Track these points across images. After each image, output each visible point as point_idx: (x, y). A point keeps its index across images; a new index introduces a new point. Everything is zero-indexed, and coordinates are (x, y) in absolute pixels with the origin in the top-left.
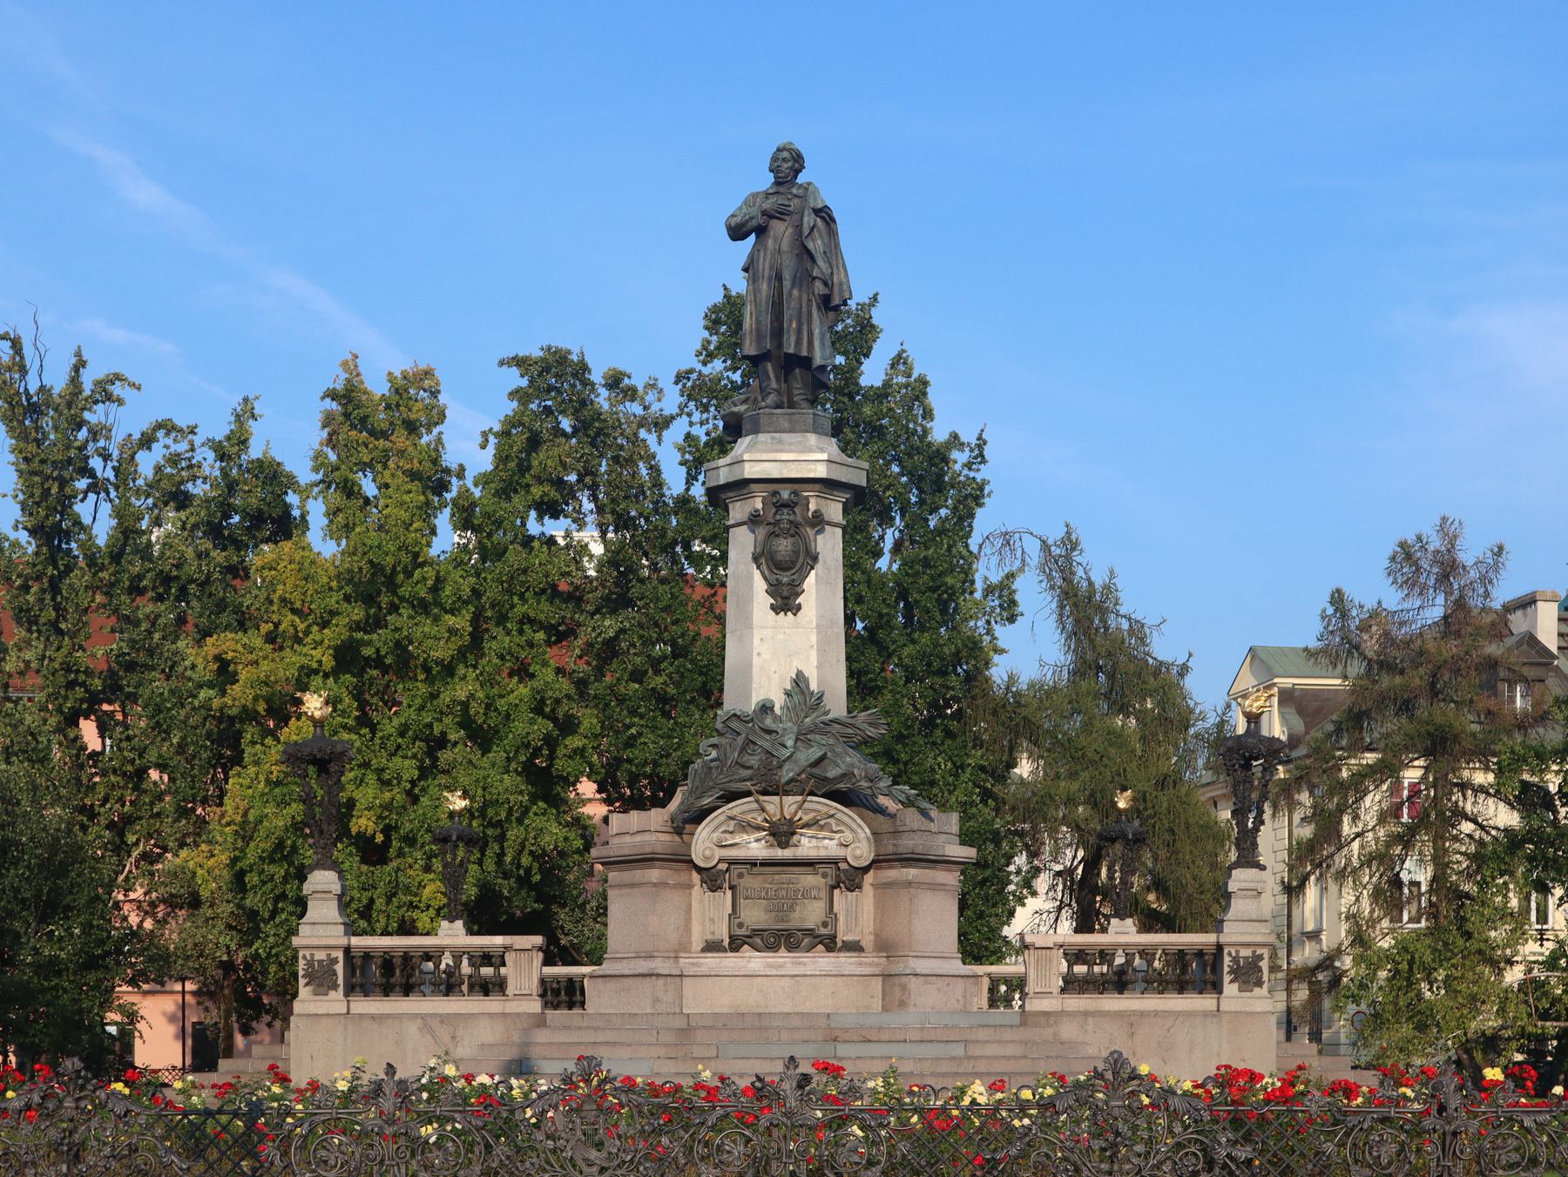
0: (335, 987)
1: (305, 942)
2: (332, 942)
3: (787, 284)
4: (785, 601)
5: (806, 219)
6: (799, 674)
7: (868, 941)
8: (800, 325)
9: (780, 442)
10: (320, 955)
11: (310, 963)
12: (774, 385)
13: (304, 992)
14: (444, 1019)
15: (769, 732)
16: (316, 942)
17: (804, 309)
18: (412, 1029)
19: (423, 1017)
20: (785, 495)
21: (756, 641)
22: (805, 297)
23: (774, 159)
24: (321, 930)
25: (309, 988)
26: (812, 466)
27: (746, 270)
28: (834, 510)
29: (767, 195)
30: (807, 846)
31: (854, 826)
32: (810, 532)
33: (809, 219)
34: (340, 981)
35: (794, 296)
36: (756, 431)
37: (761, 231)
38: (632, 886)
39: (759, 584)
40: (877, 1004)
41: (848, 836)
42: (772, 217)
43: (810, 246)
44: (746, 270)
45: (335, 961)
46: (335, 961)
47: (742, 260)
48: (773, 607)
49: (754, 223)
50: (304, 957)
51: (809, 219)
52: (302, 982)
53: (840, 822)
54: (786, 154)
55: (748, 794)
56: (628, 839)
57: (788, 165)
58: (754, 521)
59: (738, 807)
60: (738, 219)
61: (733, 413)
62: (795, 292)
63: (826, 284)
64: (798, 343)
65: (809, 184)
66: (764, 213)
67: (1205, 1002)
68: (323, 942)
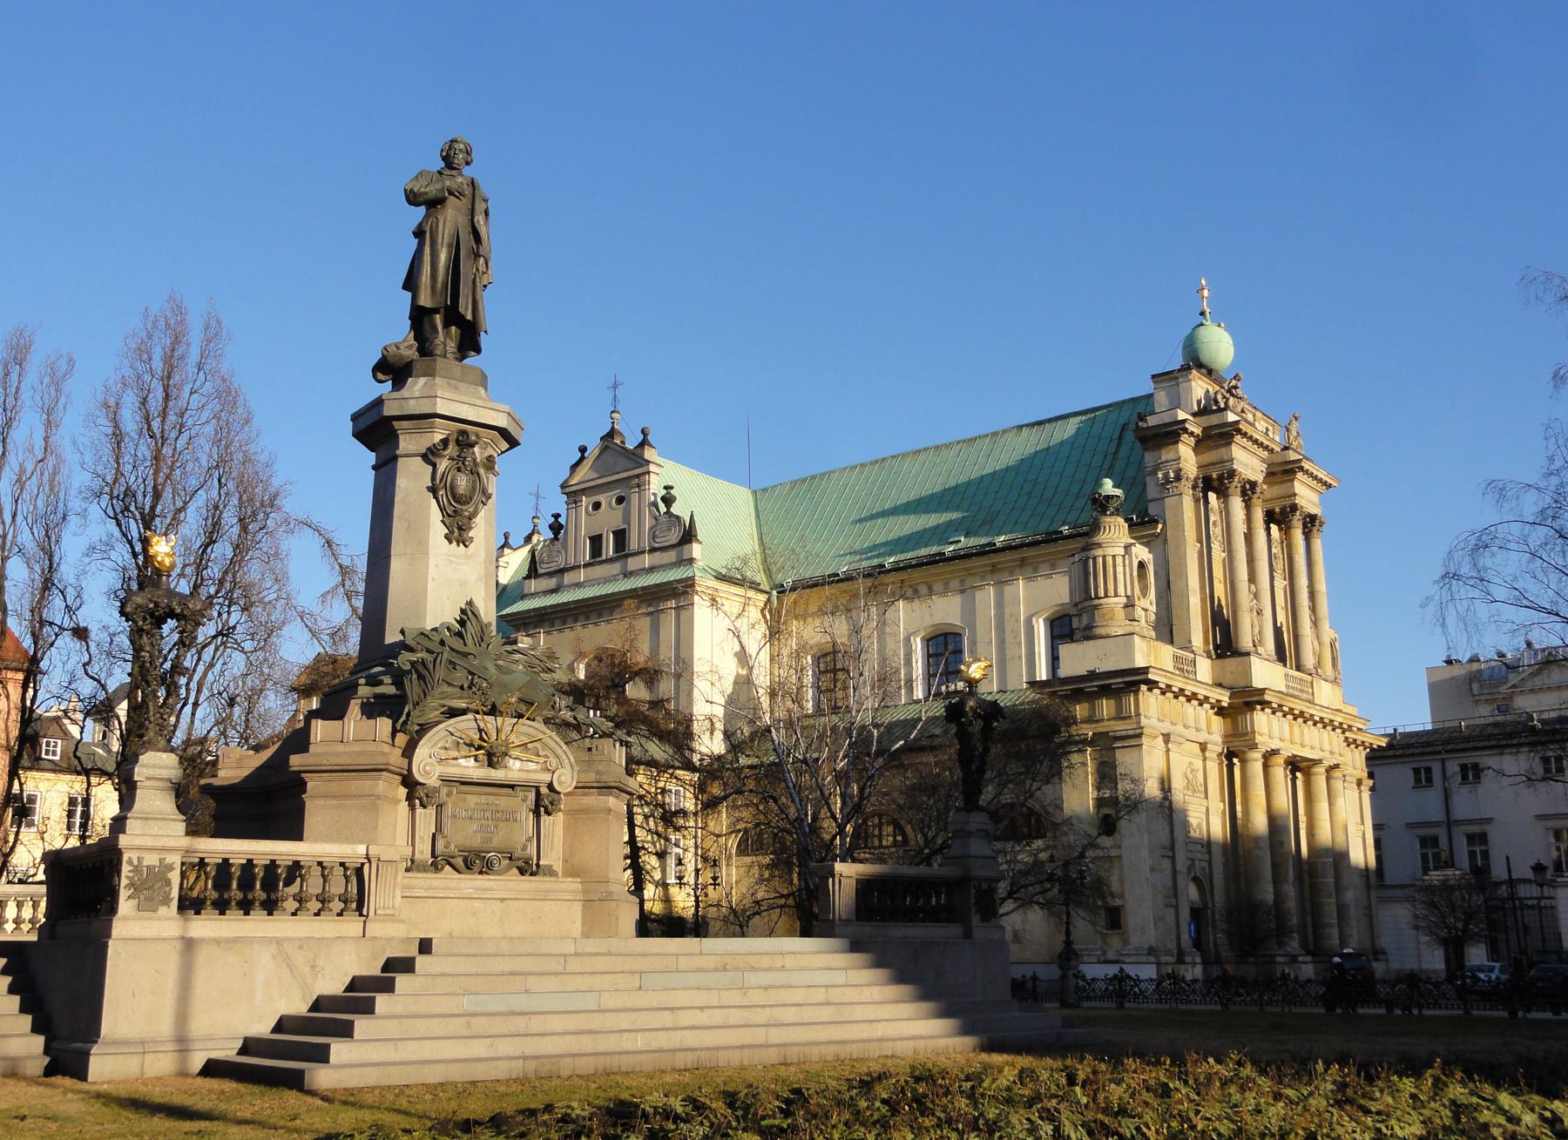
0: (166, 901)
1: (137, 842)
2: (171, 843)
3: (462, 253)
4: (458, 532)
6: (470, 603)
7: (558, 866)
9: (456, 388)
10: (151, 860)
11: (137, 869)
13: (125, 906)
14: (302, 943)
15: (465, 655)
16: (150, 842)
18: (265, 957)
19: (279, 942)
21: (431, 566)
24: (155, 828)
25: (134, 902)
26: (493, 413)
30: (516, 769)
31: (559, 751)
34: (175, 894)
37: (435, 204)
38: (346, 796)
39: (435, 514)
40: (577, 929)
41: (554, 762)
42: (451, 193)
45: (171, 868)
46: (171, 868)
48: (446, 537)
50: (130, 862)
52: (123, 894)
53: (546, 746)
55: (464, 712)
56: (340, 748)
58: (430, 456)
59: (465, 725)
67: (954, 930)
68: (160, 843)
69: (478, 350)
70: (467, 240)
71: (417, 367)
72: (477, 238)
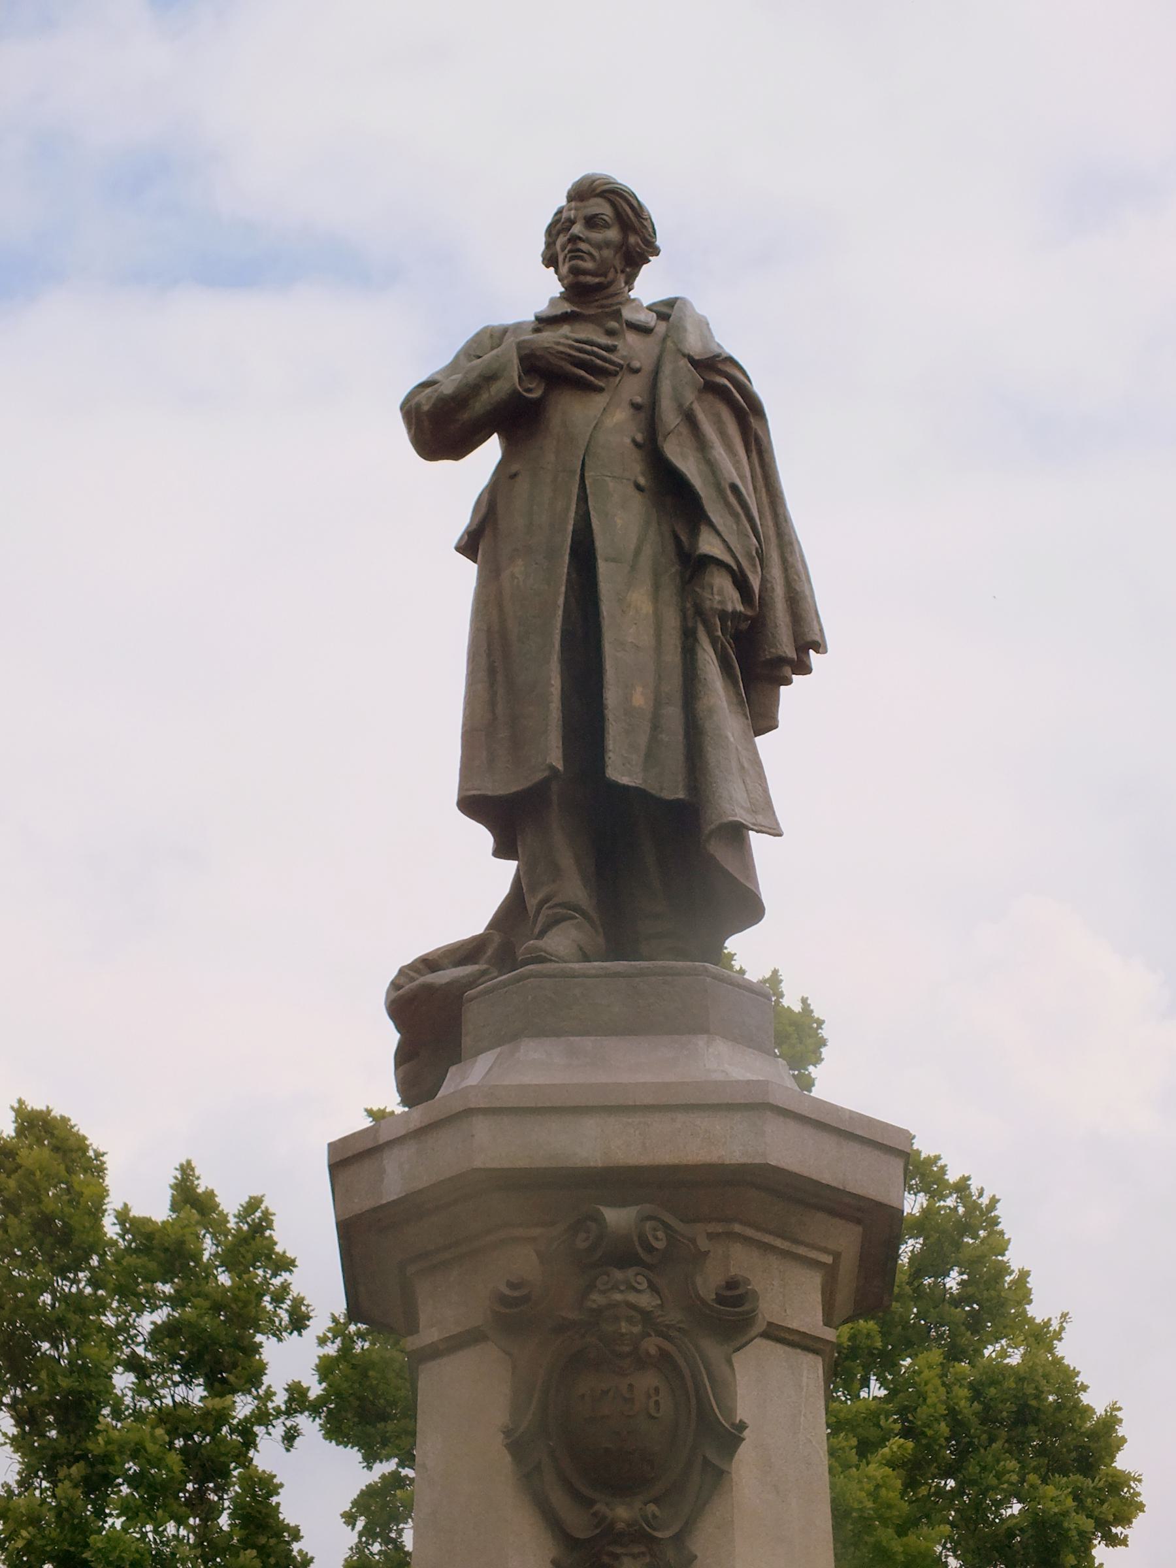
5: (666, 387)
8: (658, 702)
12: (574, 888)
17: (673, 656)
20: (617, 1218)
22: (672, 620)
23: (558, 228)
27: (469, 546)
28: (795, 1297)
29: (544, 322)
32: (713, 1350)
33: (678, 387)
35: (635, 617)
36: (507, 1036)
43: (689, 466)
44: (469, 546)
47: (461, 519)
49: (498, 391)
51: (678, 387)
54: (603, 209)
57: (602, 234)
60: (448, 388)
61: (429, 989)
62: (641, 600)
63: (741, 583)
64: (651, 757)
65: (671, 303)
66: (534, 363)
69: (748, 909)
70: (625, 523)
71: (475, 1017)
72: (673, 497)
